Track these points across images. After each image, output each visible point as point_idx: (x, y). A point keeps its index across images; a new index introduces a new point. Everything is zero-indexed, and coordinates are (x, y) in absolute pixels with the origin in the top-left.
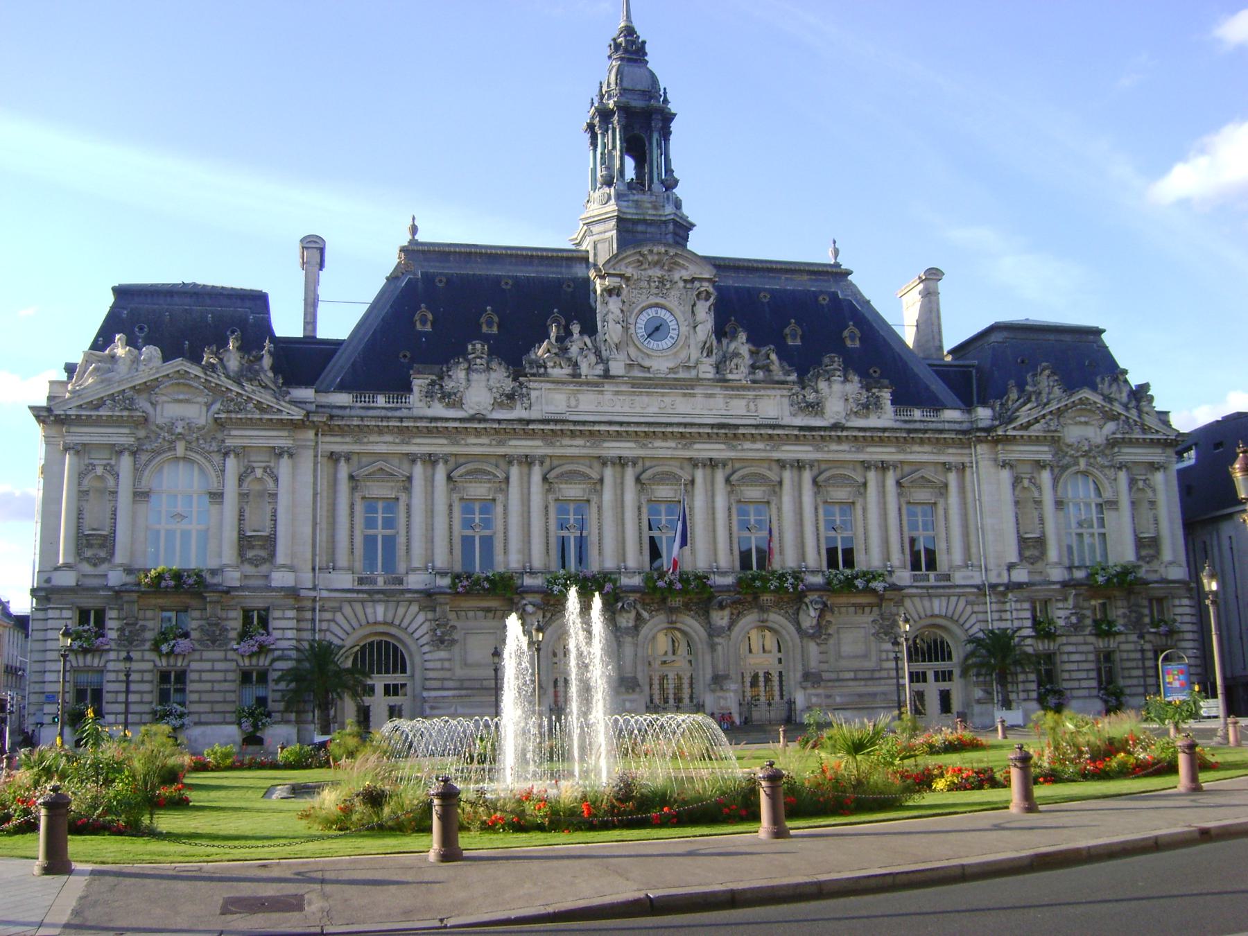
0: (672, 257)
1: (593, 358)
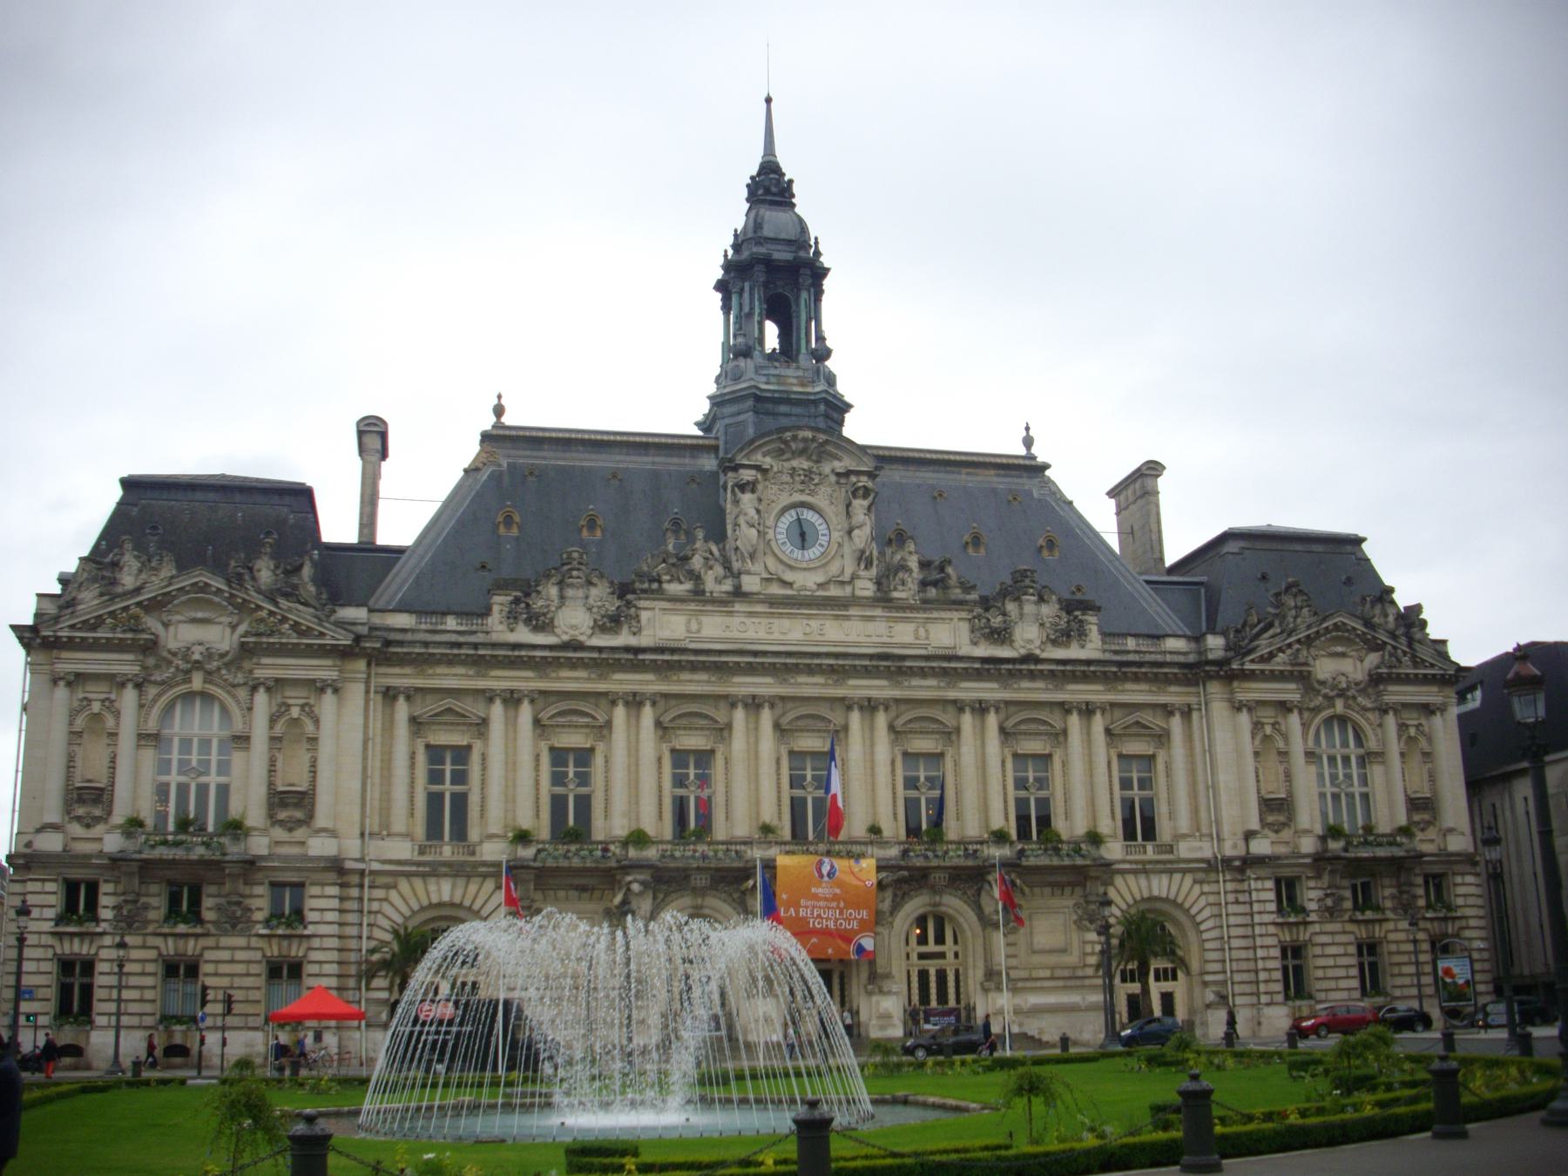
0: (821, 445)
1: (719, 570)
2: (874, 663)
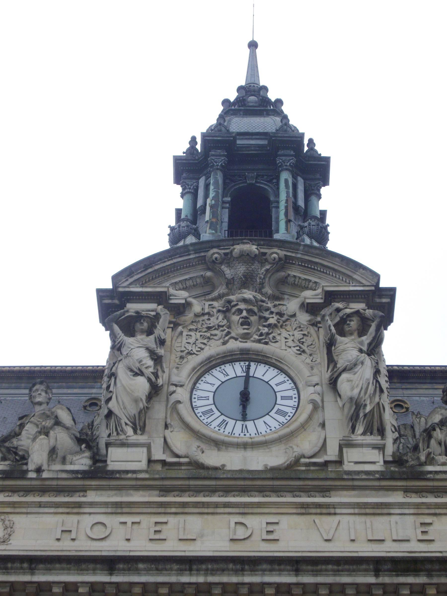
2: (386, 580)
